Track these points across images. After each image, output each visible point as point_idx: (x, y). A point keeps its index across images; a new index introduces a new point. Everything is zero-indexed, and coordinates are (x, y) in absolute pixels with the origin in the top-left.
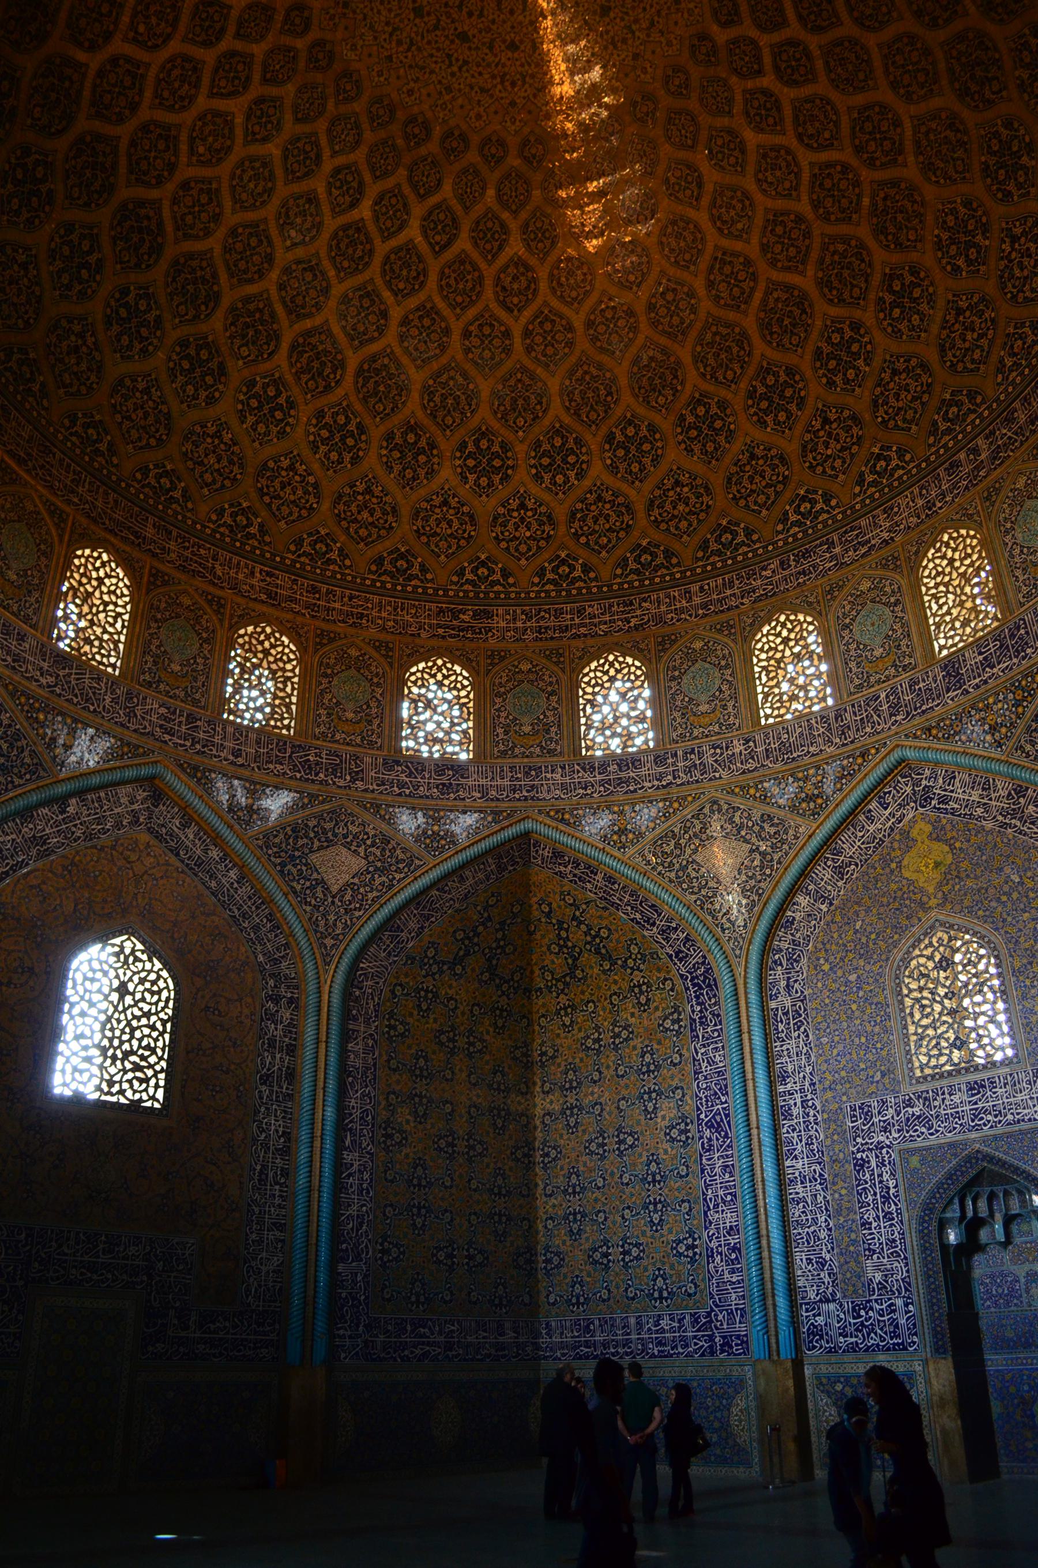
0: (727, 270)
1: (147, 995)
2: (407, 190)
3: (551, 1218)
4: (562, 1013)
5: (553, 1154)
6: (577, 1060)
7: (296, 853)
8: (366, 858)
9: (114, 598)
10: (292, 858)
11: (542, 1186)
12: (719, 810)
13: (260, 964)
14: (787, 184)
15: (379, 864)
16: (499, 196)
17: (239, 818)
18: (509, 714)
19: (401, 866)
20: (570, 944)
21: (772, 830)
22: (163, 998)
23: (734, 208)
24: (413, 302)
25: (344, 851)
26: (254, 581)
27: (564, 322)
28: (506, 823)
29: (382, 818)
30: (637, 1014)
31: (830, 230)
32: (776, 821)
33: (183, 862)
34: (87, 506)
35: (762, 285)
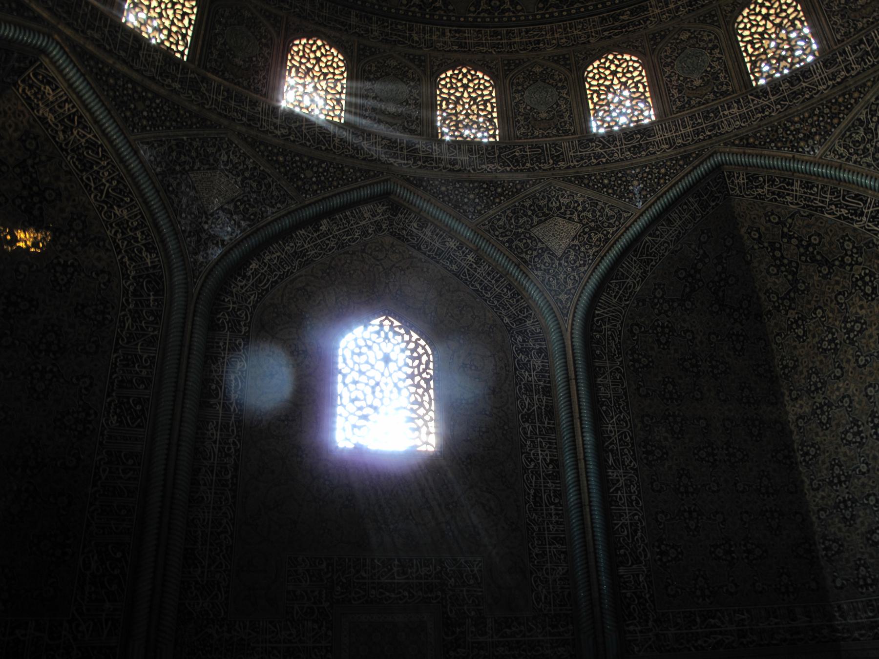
1: (410, 362)
3: (822, 509)
4: (794, 326)
5: (812, 451)
6: (818, 363)
7: (520, 230)
8: (580, 221)
9: (332, 70)
10: (517, 235)
11: (808, 482)
13: (507, 325)
15: (593, 224)
17: (465, 211)
18: (679, 76)
19: (612, 221)
20: (786, 261)
22: (424, 361)
25: (560, 220)
26: (446, 39)
28: (696, 162)
29: (587, 186)
30: (866, 305)
33: (425, 254)
34: (297, 10)
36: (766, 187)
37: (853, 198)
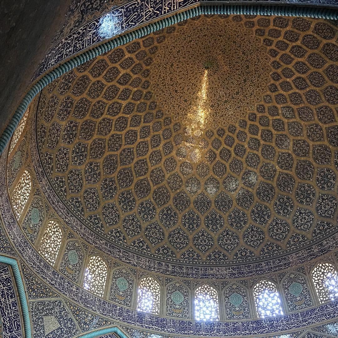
0: (143, 165)
2: (133, 65)
12: (60, 306)
14: (169, 168)
16: (135, 92)
21: (70, 326)
23: (157, 158)
24: (104, 82)
27: (110, 128)
31: (167, 186)
32: (73, 323)
35: (145, 177)
36: (5, 288)
37: (17, 325)
